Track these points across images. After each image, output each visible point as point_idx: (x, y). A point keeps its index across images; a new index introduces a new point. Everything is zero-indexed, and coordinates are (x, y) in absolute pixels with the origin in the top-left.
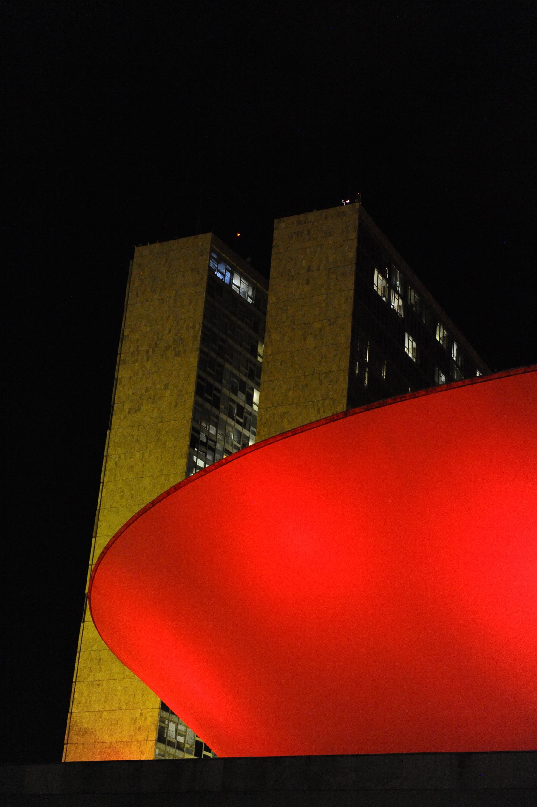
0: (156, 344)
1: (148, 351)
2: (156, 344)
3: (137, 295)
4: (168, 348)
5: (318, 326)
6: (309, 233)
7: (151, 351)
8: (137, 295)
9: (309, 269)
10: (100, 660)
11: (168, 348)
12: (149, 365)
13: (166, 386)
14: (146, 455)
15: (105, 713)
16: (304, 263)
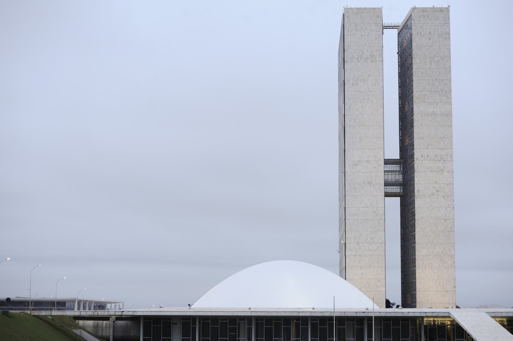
0: (361, 55)
1: (358, 58)
2: (361, 55)
3: (349, 31)
4: (368, 58)
5: (436, 59)
6: (428, 17)
7: (359, 58)
8: (349, 31)
9: (430, 34)
10: (355, 188)
11: (368, 58)
12: (359, 64)
13: (369, 76)
14: (364, 105)
15: (361, 209)
16: (427, 30)
